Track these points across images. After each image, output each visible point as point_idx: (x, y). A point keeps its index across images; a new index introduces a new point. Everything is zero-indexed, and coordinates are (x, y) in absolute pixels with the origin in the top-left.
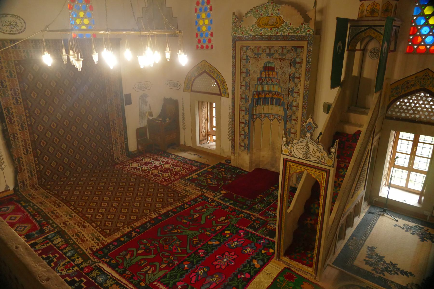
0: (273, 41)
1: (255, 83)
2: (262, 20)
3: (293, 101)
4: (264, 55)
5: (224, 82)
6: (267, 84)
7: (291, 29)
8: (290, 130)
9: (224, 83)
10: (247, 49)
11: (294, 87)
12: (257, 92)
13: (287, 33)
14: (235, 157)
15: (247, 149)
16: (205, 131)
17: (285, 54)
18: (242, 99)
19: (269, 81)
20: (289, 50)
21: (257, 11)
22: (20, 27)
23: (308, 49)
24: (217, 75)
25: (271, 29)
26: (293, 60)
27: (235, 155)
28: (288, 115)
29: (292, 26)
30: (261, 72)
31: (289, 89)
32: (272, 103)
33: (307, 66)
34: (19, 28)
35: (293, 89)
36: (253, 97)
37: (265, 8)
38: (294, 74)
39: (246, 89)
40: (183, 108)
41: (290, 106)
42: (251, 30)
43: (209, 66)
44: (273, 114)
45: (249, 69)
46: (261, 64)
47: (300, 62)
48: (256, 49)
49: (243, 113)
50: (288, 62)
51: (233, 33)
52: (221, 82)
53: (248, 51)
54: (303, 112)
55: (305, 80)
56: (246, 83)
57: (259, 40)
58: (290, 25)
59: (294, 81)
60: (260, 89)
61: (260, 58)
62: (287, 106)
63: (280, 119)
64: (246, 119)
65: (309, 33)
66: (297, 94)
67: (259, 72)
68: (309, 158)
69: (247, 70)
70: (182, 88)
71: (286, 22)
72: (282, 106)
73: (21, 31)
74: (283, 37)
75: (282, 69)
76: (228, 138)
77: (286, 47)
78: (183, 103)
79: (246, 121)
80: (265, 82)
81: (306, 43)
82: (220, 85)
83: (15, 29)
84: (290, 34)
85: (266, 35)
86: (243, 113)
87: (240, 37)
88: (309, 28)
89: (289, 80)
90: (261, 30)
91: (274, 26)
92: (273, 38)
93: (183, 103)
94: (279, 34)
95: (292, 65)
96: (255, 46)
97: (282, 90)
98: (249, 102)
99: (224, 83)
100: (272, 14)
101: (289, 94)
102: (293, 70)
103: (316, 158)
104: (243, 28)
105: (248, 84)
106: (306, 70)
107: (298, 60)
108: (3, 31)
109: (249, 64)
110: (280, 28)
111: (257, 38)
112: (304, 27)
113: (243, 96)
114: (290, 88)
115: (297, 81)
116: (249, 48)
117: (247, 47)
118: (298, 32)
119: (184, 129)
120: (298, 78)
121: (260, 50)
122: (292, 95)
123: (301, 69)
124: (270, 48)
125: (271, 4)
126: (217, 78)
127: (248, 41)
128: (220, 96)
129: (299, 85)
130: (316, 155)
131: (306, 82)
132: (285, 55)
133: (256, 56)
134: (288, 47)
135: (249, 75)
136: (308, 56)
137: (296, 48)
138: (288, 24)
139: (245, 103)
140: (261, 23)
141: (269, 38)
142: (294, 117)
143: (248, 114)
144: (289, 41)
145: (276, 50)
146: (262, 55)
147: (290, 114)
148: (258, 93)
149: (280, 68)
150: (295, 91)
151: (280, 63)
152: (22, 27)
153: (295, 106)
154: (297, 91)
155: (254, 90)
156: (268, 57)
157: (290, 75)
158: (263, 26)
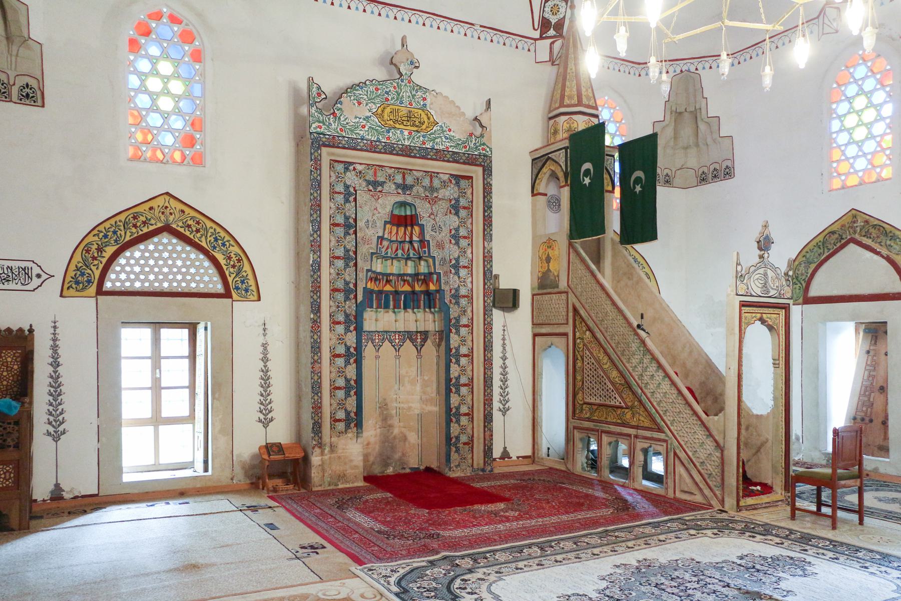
0: (415, 157)
1: (371, 251)
2: (388, 110)
3: (459, 286)
4: (390, 187)
7: (451, 140)
10: (347, 169)
11: (459, 257)
13: (443, 147)
15: (356, 425)
17: (436, 189)
20: (444, 182)
21: (377, 89)
23: (486, 182)
24: (216, 239)
25: (410, 133)
26: (453, 202)
29: (452, 133)
30: (386, 223)
31: (450, 260)
33: (486, 214)
35: (457, 260)
37: (395, 88)
38: (457, 230)
42: (364, 127)
43: (183, 211)
46: (386, 205)
47: (467, 205)
48: (371, 172)
49: (340, 329)
50: (443, 206)
53: (348, 174)
58: (448, 133)
59: (457, 243)
61: (379, 191)
63: (397, 341)
65: (484, 152)
67: (380, 224)
68: (768, 292)
71: (440, 124)
74: (436, 153)
75: (434, 219)
76: (260, 421)
77: (438, 173)
78: (55, 340)
81: (480, 169)
82: (225, 267)
84: (450, 150)
88: (484, 144)
91: (415, 129)
92: (415, 151)
93: (55, 340)
94: (428, 147)
97: (437, 263)
100: (410, 104)
101: (451, 270)
102: (454, 221)
103: (775, 289)
105: (351, 253)
107: (463, 202)
110: (430, 135)
112: (476, 140)
113: (340, 285)
114: (451, 257)
116: (351, 168)
117: (347, 165)
118: (465, 147)
120: (465, 237)
121: (379, 174)
122: (457, 273)
124: (404, 172)
125: (408, 84)
126: (215, 247)
129: (469, 251)
130: (775, 285)
132: (437, 190)
133: (371, 188)
135: (355, 233)
137: (458, 178)
138: (445, 129)
139: (345, 301)
140: (386, 117)
141: (407, 152)
142: (464, 321)
143: (355, 329)
144: (448, 161)
145: (418, 179)
148: (376, 277)
149: (429, 217)
151: (428, 205)
153: (464, 296)
155: (369, 268)
156: (400, 191)
158: (391, 122)
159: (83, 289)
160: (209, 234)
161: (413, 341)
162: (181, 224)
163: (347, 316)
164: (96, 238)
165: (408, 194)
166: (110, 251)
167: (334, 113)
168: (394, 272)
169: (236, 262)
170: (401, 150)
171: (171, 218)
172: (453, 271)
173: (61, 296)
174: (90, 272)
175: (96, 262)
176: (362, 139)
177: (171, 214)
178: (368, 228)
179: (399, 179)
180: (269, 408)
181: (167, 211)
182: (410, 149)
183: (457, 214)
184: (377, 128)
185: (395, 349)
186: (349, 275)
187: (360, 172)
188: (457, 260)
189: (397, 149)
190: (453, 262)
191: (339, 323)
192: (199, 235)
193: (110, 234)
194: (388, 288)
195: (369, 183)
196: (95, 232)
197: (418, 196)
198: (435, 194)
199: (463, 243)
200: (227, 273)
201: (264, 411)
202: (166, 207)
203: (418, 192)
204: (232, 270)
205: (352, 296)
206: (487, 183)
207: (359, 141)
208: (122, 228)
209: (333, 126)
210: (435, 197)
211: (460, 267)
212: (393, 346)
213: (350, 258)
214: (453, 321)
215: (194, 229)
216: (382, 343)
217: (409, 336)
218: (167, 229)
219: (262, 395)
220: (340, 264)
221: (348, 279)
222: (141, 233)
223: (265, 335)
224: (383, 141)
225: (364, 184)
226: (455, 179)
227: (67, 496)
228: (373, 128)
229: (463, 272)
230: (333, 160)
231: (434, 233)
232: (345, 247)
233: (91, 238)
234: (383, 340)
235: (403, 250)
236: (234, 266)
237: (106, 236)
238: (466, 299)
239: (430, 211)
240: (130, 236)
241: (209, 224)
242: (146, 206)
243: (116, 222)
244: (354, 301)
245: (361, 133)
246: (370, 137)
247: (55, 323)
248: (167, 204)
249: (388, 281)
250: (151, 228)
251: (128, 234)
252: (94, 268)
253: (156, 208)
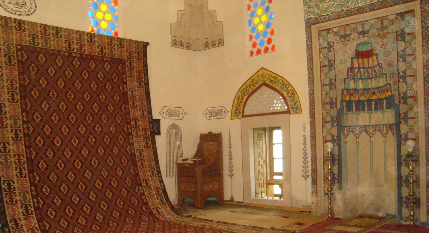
3: (406, 91)
4: (355, 35)
5: (294, 92)
6: (361, 78)
8: (406, 135)
9: (293, 94)
10: (328, 33)
11: (406, 70)
12: (348, 90)
14: (319, 199)
15: (338, 182)
16: (262, 178)
17: (386, 27)
18: (326, 105)
19: (364, 73)
20: (392, 20)
22: (29, 8)
24: (283, 85)
26: (399, 32)
27: (319, 195)
28: (401, 112)
30: (352, 59)
31: (399, 73)
32: (370, 109)
34: (27, 9)
35: (404, 72)
36: (342, 98)
39: (331, 89)
40: (230, 144)
41: (404, 98)
42: (333, 6)
43: (269, 75)
44: (372, 126)
45: (333, 59)
48: (342, 30)
49: (328, 126)
50: (392, 37)
51: (306, 16)
52: (289, 93)
53: (329, 36)
54: (426, 101)
55: (423, 53)
56: (331, 80)
57: (345, 15)
60: (352, 86)
61: (348, 40)
62: (398, 98)
64: (333, 134)
66: (412, 78)
69: (330, 61)
70: (229, 115)
72: (387, 108)
73: (30, 13)
75: (385, 48)
76: (303, 176)
77: (386, 16)
78: (230, 137)
79: (333, 137)
80: (359, 75)
82: (287, 98)
83: (23, 10)
85: (356, 6)
86: (328, 126)
87: (317, 18)
89: (396, 61)
90: (348, 3)
92: (366, 8)
93: (230, 137)
95: (400, 39)
96: (340, 26)
97: (388, 77)
98: (336, 106)
99: (293, 94)
101: (399, 81)
102: (401, 45)
104: (321, 6)
106: (423, 39)
108: (8, 10)
109: (333, 52)
111: (342, 13)
113: (328, 100)
114: (400, 71)
115: (409, 59)
116: (331, 31)
117: (328, 31)
119: (231, 176)
120: (410, 55)
122: (405, 82)
123: (414, 42)
126: (282, 89)
127: (329, 20)
128: (288, 114)
129: (414, 65)
131: (425, 56)
132: (386, 28)
133: (343, 39)
134: (389, 17)
135: (335, 68)
136: (423, 19)
142: (411, 114)
143: (337, 125)
144: (391, 6)
145: (372, 25)
146: (352, 36)
147: (405, 111)
149: (381, 47)
150: (408, 74)
151: (380, 40)
152: (31, 8)
153: (411, 97)
154: (412, 74)
155: (343, 88)
156: (361, 36)
157: (398, 53)
159: (238, 115)
160: (280, 83)
161: (392, 130)
162: (269, 81)
163: (332, 118)
165: (366, 37)
166: (245, 98)
167: (316, 5)
168: (374, 87)
170: (357, 11)
171: (265, 79)
172: (401, 80)
173: (231, 119)
175: (241, 104)
176: (333, 13)
178: (341, 64)
179: (360, 29)
180: (307, 170)
181: (264, 76)
182: (363, 8)
183: (403, 40)
184: (341, 3)
185: (384, 136)
186: (332, 94)
187: (336, 32)
188: (404, 72)
189: (354, 11)
190: (401, 74)
191: (327, 122)
192: (276, 84)
193: (245, 91)
194: (374, 97)
195: (341, 37)
197: (373, 36)
198: (385, 31)
199: (409, 59)
200: (288, 101)
201: (305, 171)
202: (263, 74)
203: (373, 33)
204: (290, 99)
205: (334, 106)
206: (424, 11)
207: (331, 15)
208: (249, 87)
209: (316, 12)
210: (386, 33)
211: (407, 77)
212: (382, 134)
213: (332, 84)
214: (403, 116)
215: (274, 82)
216: (375, 132)
217: (377, 127)
218: (264, 84)
219: (304, 163)
220: (327, 88)
221: (332, 96)
222: (255, 88)
223: (304, 131)
224: (345, 9)
225: (338, 38)
226: (400, 16)
227: (235, 200)
228: (338, 4)
229: (409, 80)
230: (321, 31)
231: (385, 58)
232: (329, 78)
234: (375, 131)
235: (368, 72)
236: (291, 97)
237: (244, 92)
238: (413, 99)
239: (382, 43)
241: (280, 78)
244: (336, 108)
245: (332, 10)
246: (337, 10)
247: (229, 130)
248: (263, 73)
249: (374, 93)
250: (259, 85)
251: (251, 89)
252: (241, 106)
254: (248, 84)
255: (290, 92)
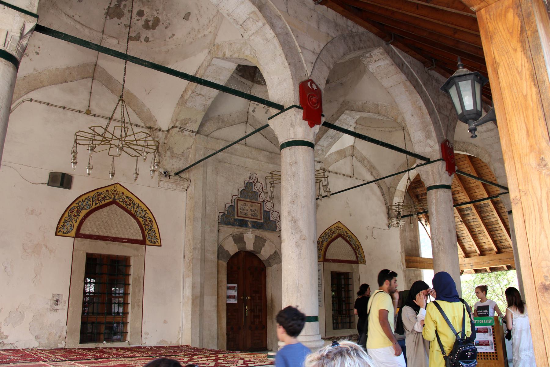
162: (121, 200)
164: (77, 205)
166: (83, 213)
169: (149, 223)
171: (117, 197)
174: (72, 223)
175: (75, 218)
177: (117, 194)
192: (130, 207)
196: (77, 202)
204: (147, 227)
208: (91, 200)
215: (128, 203)
218: (114, 202)
222: (101, 204)
233: (74, 205)
236: (148, 225)
240: (95, 205)
242: (105, 190)
243: (88, 197)
250: (107, 201)
251: (94, 204)
252: (74, 222)
253: (110, 191)
254: (91, 197)
255: (148, 220)
